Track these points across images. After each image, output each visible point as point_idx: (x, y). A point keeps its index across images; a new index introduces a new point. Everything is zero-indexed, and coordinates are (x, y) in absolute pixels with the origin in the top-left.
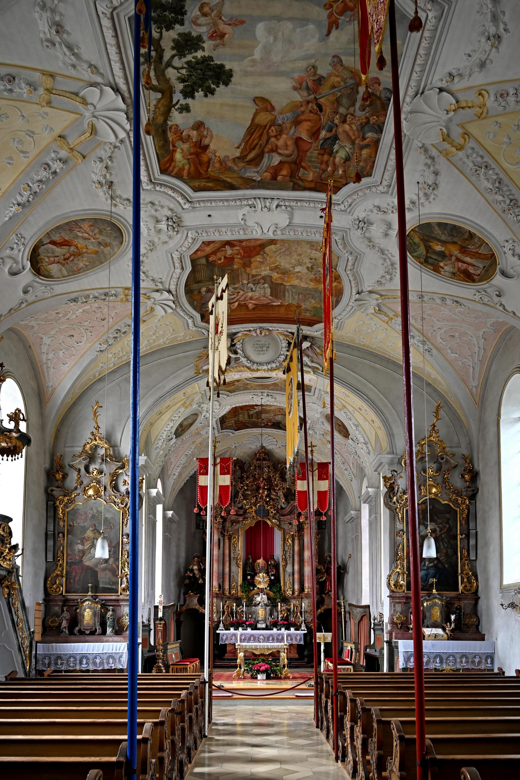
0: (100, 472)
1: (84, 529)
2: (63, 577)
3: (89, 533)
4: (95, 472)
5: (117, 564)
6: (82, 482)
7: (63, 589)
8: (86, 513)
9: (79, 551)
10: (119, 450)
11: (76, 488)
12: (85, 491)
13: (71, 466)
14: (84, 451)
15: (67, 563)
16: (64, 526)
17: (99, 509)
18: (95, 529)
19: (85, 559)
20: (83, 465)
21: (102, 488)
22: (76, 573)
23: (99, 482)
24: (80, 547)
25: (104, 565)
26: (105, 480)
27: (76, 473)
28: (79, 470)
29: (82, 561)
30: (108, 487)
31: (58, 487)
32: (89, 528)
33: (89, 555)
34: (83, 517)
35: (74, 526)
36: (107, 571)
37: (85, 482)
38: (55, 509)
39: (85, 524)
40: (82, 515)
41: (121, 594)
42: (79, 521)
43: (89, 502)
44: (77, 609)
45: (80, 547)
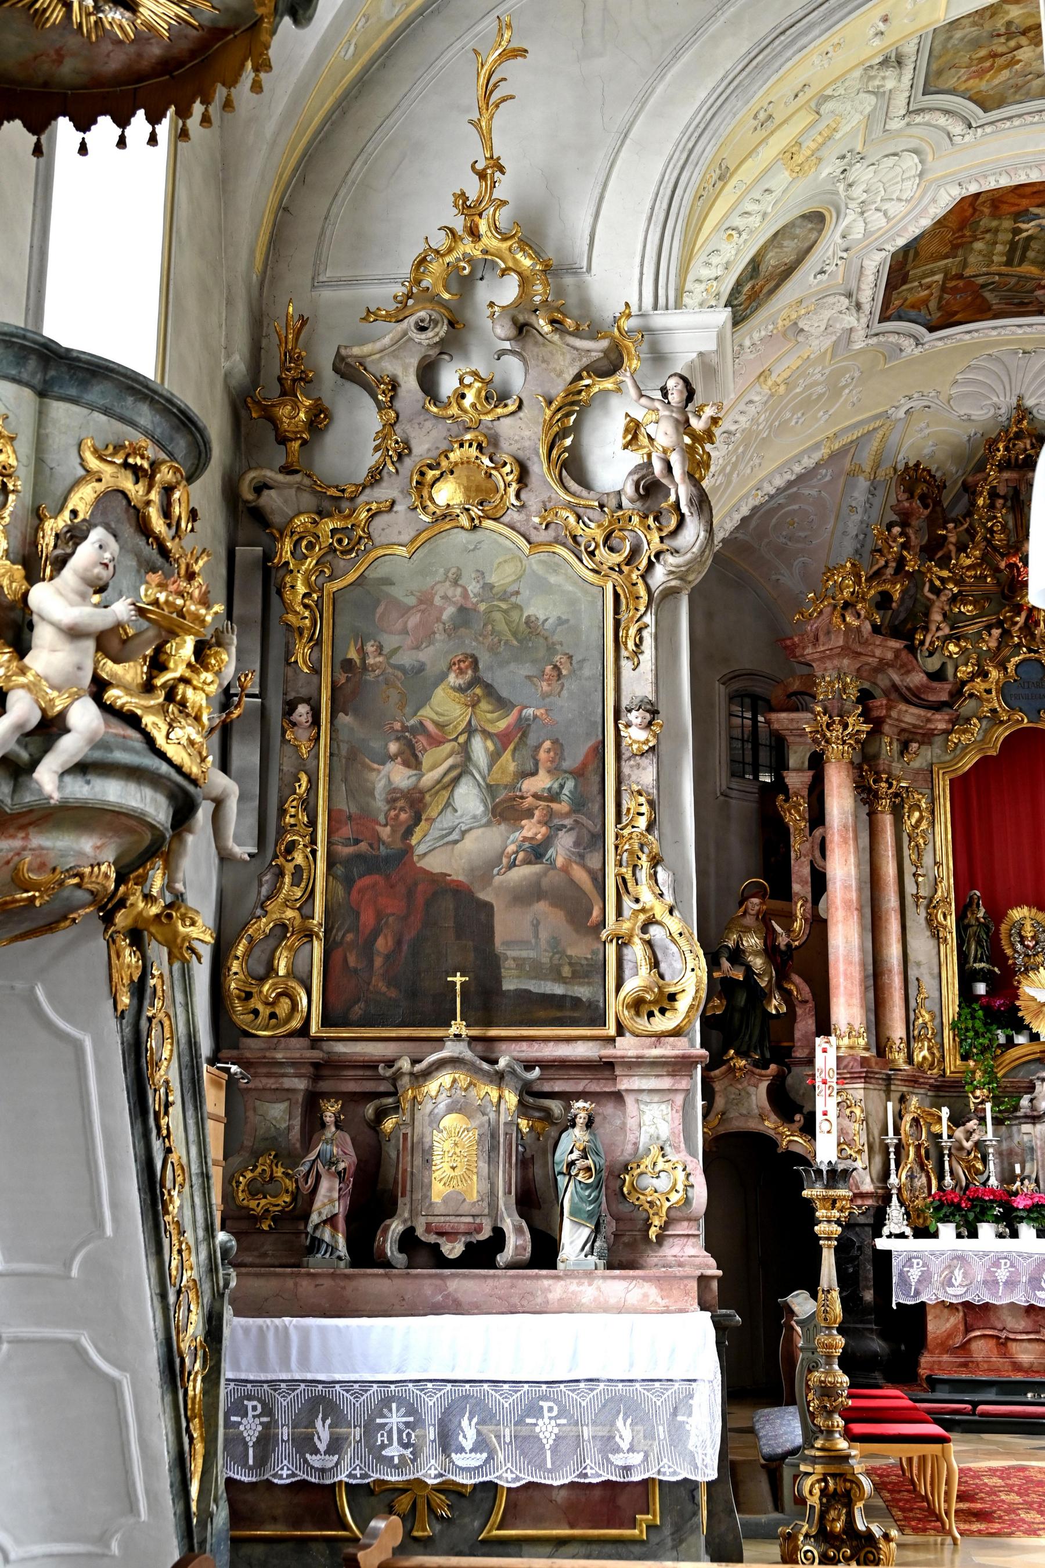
0: (496, 395)
1: (419, 684)
2: (309, 935)
3: (446, 705)
5: (594, 863)
7: (311, 1003)
8: (425, 600)
9: (394, 797)
10: (581, 287)
11: (376, 477)
12: (422, 486)
13: (349, 370)
14: (415, 293)
16: (316, 671)
17: (493, 579)
18: (476, 681)
19: (422, 841)
20: (414, 362)
21: (509, 473)
22: (379, 915)
23: (489, 444)
24: (400, 776)
25: (523, 872)
26: (524, 432)
29: (409, 850)
30: (539, 468)
31: (288, 470)
32: (443, 677)
33: (447, 820)
34: (413, 620)
35: (365, 667)
36: (542, 906)
37: (422, 447)
38: (271, 578)
39: (425, 655)
40: (407, 610)
41: (621, 1030)
42: (390, 641)
43: (443, 541)
44: (382, 1114)
45: (400, 776)
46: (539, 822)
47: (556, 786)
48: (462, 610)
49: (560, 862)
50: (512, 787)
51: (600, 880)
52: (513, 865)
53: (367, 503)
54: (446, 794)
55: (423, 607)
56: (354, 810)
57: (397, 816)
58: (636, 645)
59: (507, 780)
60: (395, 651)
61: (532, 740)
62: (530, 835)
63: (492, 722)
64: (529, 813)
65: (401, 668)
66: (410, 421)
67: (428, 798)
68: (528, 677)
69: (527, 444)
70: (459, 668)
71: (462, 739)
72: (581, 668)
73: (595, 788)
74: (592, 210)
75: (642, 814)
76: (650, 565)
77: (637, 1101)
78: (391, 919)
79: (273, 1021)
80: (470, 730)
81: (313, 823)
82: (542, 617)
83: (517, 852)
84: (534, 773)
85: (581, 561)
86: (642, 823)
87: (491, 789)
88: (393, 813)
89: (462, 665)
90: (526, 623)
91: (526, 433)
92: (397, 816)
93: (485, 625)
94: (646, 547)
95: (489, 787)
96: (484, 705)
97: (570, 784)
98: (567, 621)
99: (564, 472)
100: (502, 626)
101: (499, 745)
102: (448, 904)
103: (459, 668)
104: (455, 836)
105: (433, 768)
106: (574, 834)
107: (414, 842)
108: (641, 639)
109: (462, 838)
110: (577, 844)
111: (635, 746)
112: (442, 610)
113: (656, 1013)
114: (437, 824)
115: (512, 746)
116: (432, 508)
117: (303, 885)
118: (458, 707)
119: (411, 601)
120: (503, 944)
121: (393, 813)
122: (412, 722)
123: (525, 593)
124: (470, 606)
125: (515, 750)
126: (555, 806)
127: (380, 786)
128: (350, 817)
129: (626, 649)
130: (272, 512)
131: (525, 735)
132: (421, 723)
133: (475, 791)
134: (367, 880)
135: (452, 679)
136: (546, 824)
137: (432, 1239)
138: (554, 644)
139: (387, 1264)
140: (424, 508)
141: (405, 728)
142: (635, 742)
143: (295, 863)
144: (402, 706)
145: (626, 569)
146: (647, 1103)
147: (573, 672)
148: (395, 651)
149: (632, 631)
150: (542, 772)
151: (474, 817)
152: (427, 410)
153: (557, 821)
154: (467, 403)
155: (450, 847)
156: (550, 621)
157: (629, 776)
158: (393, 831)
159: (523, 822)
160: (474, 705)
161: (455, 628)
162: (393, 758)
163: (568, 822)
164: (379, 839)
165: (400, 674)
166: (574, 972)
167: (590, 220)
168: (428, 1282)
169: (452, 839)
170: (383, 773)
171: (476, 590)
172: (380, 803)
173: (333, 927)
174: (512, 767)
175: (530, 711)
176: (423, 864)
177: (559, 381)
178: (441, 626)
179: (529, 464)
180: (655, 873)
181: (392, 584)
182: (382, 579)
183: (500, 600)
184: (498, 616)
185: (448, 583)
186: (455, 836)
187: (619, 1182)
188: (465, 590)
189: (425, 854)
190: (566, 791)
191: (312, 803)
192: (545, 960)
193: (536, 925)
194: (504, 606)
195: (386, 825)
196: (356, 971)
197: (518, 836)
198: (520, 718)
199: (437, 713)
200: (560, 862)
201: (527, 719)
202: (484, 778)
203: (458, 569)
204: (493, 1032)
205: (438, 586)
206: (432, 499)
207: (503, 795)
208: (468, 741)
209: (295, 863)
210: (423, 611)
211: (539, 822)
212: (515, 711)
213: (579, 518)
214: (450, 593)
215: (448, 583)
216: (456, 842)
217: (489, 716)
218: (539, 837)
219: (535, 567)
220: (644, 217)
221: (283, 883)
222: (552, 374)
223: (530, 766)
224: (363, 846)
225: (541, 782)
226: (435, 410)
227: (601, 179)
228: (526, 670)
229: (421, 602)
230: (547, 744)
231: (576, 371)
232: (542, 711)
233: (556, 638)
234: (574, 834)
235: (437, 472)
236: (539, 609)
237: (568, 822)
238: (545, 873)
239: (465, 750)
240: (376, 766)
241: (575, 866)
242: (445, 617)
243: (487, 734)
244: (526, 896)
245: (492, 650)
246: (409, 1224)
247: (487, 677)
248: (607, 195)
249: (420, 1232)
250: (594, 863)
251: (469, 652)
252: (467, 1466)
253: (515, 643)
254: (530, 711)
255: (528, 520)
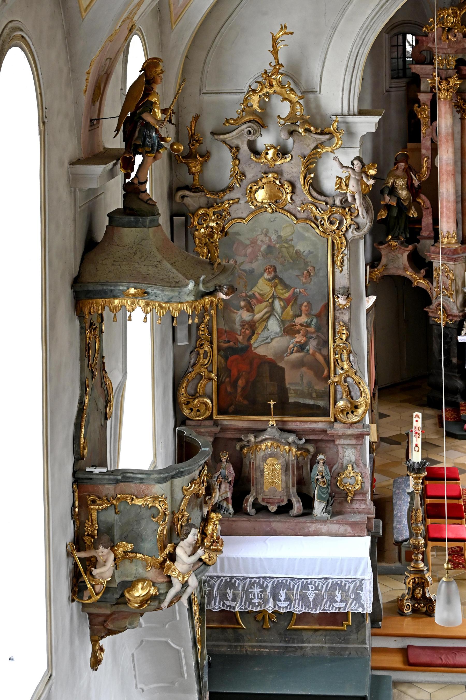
1: (252, 277)
3: (263, 286)
4: (271, 152)
5: (325, 352)
6: (244, 174)
8: (254, 242)
9: (243, 324)
10: (317, 100)
11: (230, 188)
15: (219, 350)
17: (282, 234)
23: (279, 173)
24: (246, 316)
27: (228, 155)
28: (238, 148)
29: (251, 345)
32: (262, 275)
33: (265, 334)
34: (249, 251)
36: (304, 369)
37: (250, 175)
39: (254, 265)
41: (336, 420)
45: (246, 316)
46: (302, 335)
47: (309, 321)
48: (269, 247)
49: (311, 352)
50: (291, 321)
51: (327, 359)
52: (292, 352)
53: (229, 200)
54: (264, 323)
55: (252, 245)
56: (227, 329)
57: (245, 332)
58: (341, 263)
59: (289, 318)
60: (242, 263)
61: (299, 301)
62: (299, 340)
63: (283, 294)
64: (298, 332)
65: (244, 271)
66: (245, 164)
67: (257, 324)
68: (297, 276)
69: (295, 175)
70: (269, 271)
71: (270, 301)
72: (319, 272)
73: (325, 322)
74: (321, 64)
75: (344, 334)
76: (347, 229)
77: (343, 447)
78: (244, 373)
79: (198, 413)
80: (273, 297)
81: (210, 334)
82: (302, 251)
83: (294, 347)
84: (300, 315)
85: (318, 227)
86: (344, 337)
87: (283, 322)
88: (243, 330)
89: (270, 270)
90: (296, 253)
91: (295, 170)
92: (245, 332)
93: (279, 253)
94: (345, 222)
95: (282, 321)
96: (279, 287)
97: (315, 321)
98: (313, 252)
99: (311, 188)
100: (286, 254)
101: (286, 303)
102: (266, 368)
103: (269, 271)
104: (268, 340)
105: (259, 312)
106: (316, 340)
107: (252, 342)
108: (343, 261)
109: (270, 341)
110: (318, 345)
111: (341, 306)
112: (260, 247)
113: (350, 413)
114: (261, 335)
115: (291, 304)
116: (255, 203)
117: (208, 359)
118: (268, 287)
119: (248, 242)
120: (289, 384)
121: (243, 330)
122: (250, 293)
123: (295, 240)
124: (272, 245)
125: (292, 306)
126: (308, 329)
127: (237, 319)
128: (226, 332)
129: (337, 265)
130: (189, 205)
131: (296, 300)
132: (254, 294)
133: (277, 322)
134: (234, 357)
135: (266, 276)
136: (305, 336)
137: (264, 504)
138: (307, 262)
139: (248, 514)
140: (252, 203)
141: (247, 296)
142: (340, 304)
143: (204, 349)
144: (246, 286)
145: (337, 231)
146: (346, 449)
147: (315, 274)
148: (242, 263)
149: (340, 257)
150: (303, 315)
151: (276, 333)
152: (252, 160)
153: (309, 335)
154: (269, 157)
155: (267, 345)
156: (306, 252)
157: (339, 317)
158: (244, 338)
159: (296, 335)
160: (275, 287)
161: (267, 254)
162: (242, 308)
163: (313, 336)
164: (238, 341)
165: (244, 273)
166: (317, 396)
167: (320, 69)
168: (262, 521)
169: (267, 341)
170: (238, 314)
171: (274, 239)
172: (238, 326)
173: (221, 376)
174: (291, 313)
175: (298, 290)
176: (256, 351)
177: (308, 148)
178: (261, 253)
179: (296, 183)
180: (349, 357)
181: (240, 235)
182: (235, 232)
183: (285, 243)
184: (284, 250)
185: (263, 235)
186: (268, 340)
187: (336, 481)
188: (270, 238)
189: (257, 347)
190: (313, 323)
191: (210, 324)
192: (306, 391)
193: (302, 377)
194: (286, 245)
195: (240, 335)
196: (230, 393)
197: (294, 341)
198: (294, 293)
199: (260, 290)
200: (311, 352)
201: (297, 293)
202: (280, 317)
203: (267, 229)
204: (286, 419)
205: (259, 236)
206: (256, 200)
207: (287, 324)
208: (273, 302)
209: (204, 349)
210: (253, 247)
211: (302, 335)
212: (292, 290)
213: (317, 208)
214: (264, 239)
215: (263, 235)
216: (269, 343)
217: (281, 291)
218: (303, 341)
219: (299, 229)
220: (344, 68)
221: (200, 358)
222: (305, 146)
223: (298, 313)
224: (232, 344)
225: (303, 319)
226: (255, 159)
227: (325, 50)
228: (296, 273)
229: (252, 243)
230: (305, 304)
231: (315, 145)
232: (303, 290)
233: (309, 259)
234: (316, 340)
235: (258, 187)
236: (301, 247)
237: (313, 336)
238: (305, 356)
239: (272, 305)
240: (235, 311)
241: (317, 354)
242: (262, 249)
243: (280, 299)
244: (300, 364)
245: (282, 264)
246: (255, 497)
247: (280, 275)
248: (328, 57)
249: (260, 500)
250: (325, 352)
251: (273, 264)
252: (283, 606)
253: (291, 261)
254: (298, 290)
255: (296, 208)
